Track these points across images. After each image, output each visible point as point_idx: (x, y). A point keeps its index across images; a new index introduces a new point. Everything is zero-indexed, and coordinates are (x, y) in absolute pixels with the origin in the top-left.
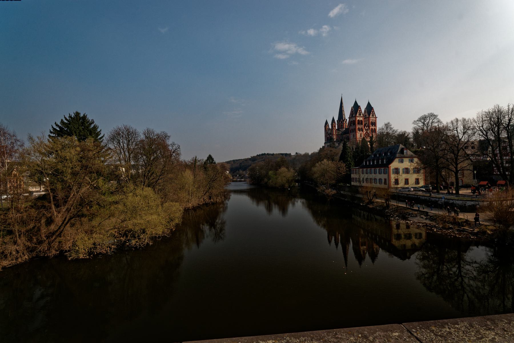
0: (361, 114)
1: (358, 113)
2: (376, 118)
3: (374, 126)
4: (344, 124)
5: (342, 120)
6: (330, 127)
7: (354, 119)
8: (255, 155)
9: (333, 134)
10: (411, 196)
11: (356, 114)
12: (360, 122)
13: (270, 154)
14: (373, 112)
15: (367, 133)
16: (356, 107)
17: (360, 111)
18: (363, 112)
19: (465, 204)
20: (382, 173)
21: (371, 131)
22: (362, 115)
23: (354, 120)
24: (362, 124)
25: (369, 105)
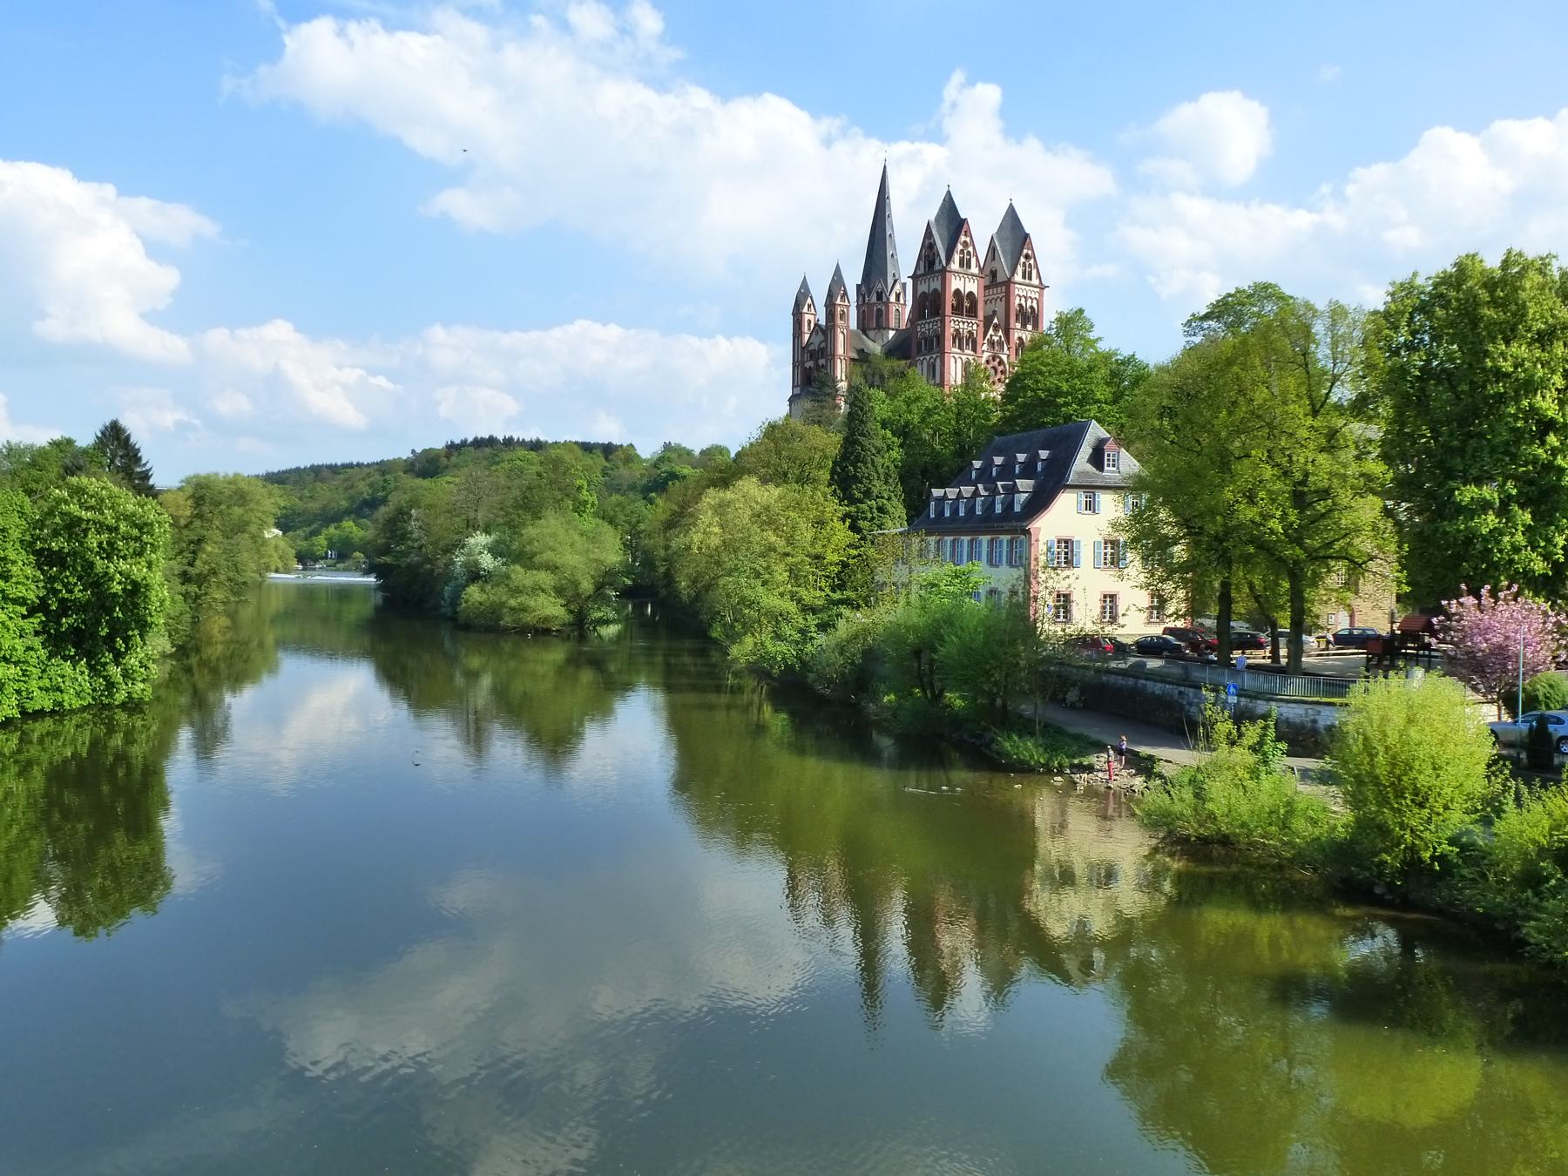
0: (973, 260)
1: (957, 257)
2: (1042, 287)
3: (1030, 327)
4: (893, 308)
5: (880, 286)
7: (936, 285)
8: (439, 444)
10: (1112, 679)
12: (966, 306)
13: (522, 443)
15: (996, 363)
17: (965, 242)
18: (982, 253)
19: (1314, 721)
20: (1000, 561)
21: (1017, 354)
22: (974, 270)
23: (935, 290)
24: (976, 316)
25: (1012, 221)
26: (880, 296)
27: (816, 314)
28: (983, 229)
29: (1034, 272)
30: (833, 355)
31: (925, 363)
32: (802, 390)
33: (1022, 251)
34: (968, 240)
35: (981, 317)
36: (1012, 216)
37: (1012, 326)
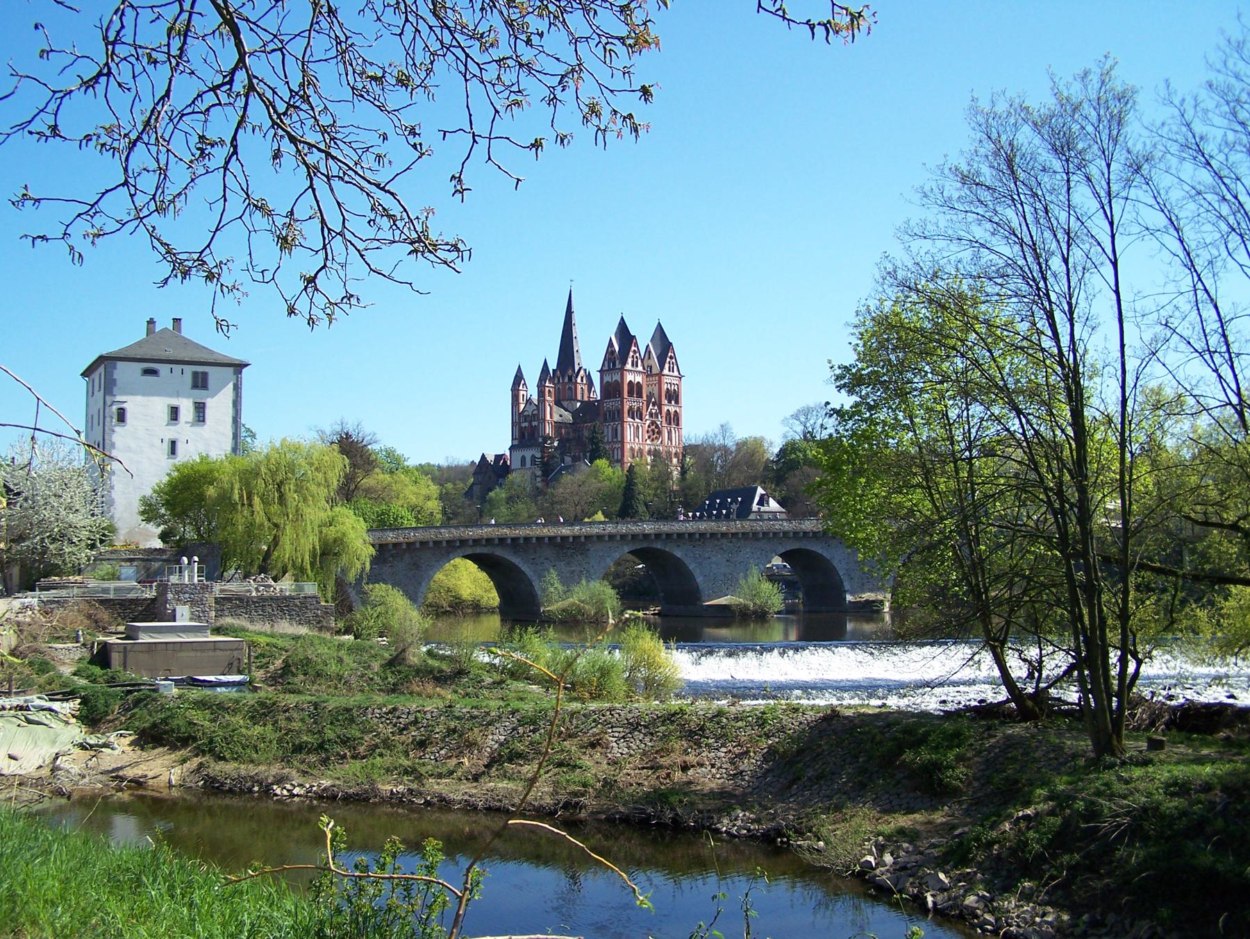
0: (639, 362)
1: (630, 360)
4: (579, 387)
5: (570, 372)
6: (533, 392)
7: (617, 377)
9: (544, 420)
11: (624, 362)
12: (635, 389)
14: (671, 358)
16: (625, 335)
22: (640, 368)
26: (570, 379)
27: (531, 390)
28: (644, 338)
32: (520, 442)
35: (645, 398)
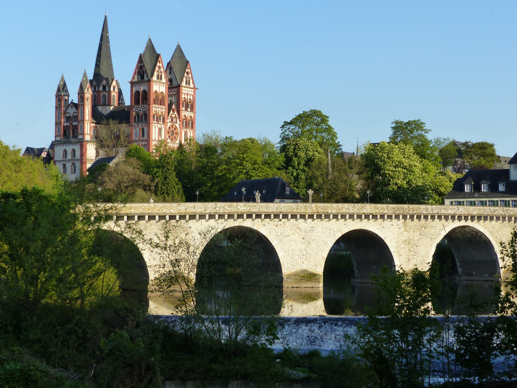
1: (156, 74)
3: (189, 110)
6: (74, 97)
22: (164, 80)
24: (164, 105)
26: (104, 88)
29: (191, 81)
30: (83, 121)
31: (138, 129)
33: (186, 70)
34: (161, 65)
35: (167, 105)
36: (179, 50)
37: (181, 109)
